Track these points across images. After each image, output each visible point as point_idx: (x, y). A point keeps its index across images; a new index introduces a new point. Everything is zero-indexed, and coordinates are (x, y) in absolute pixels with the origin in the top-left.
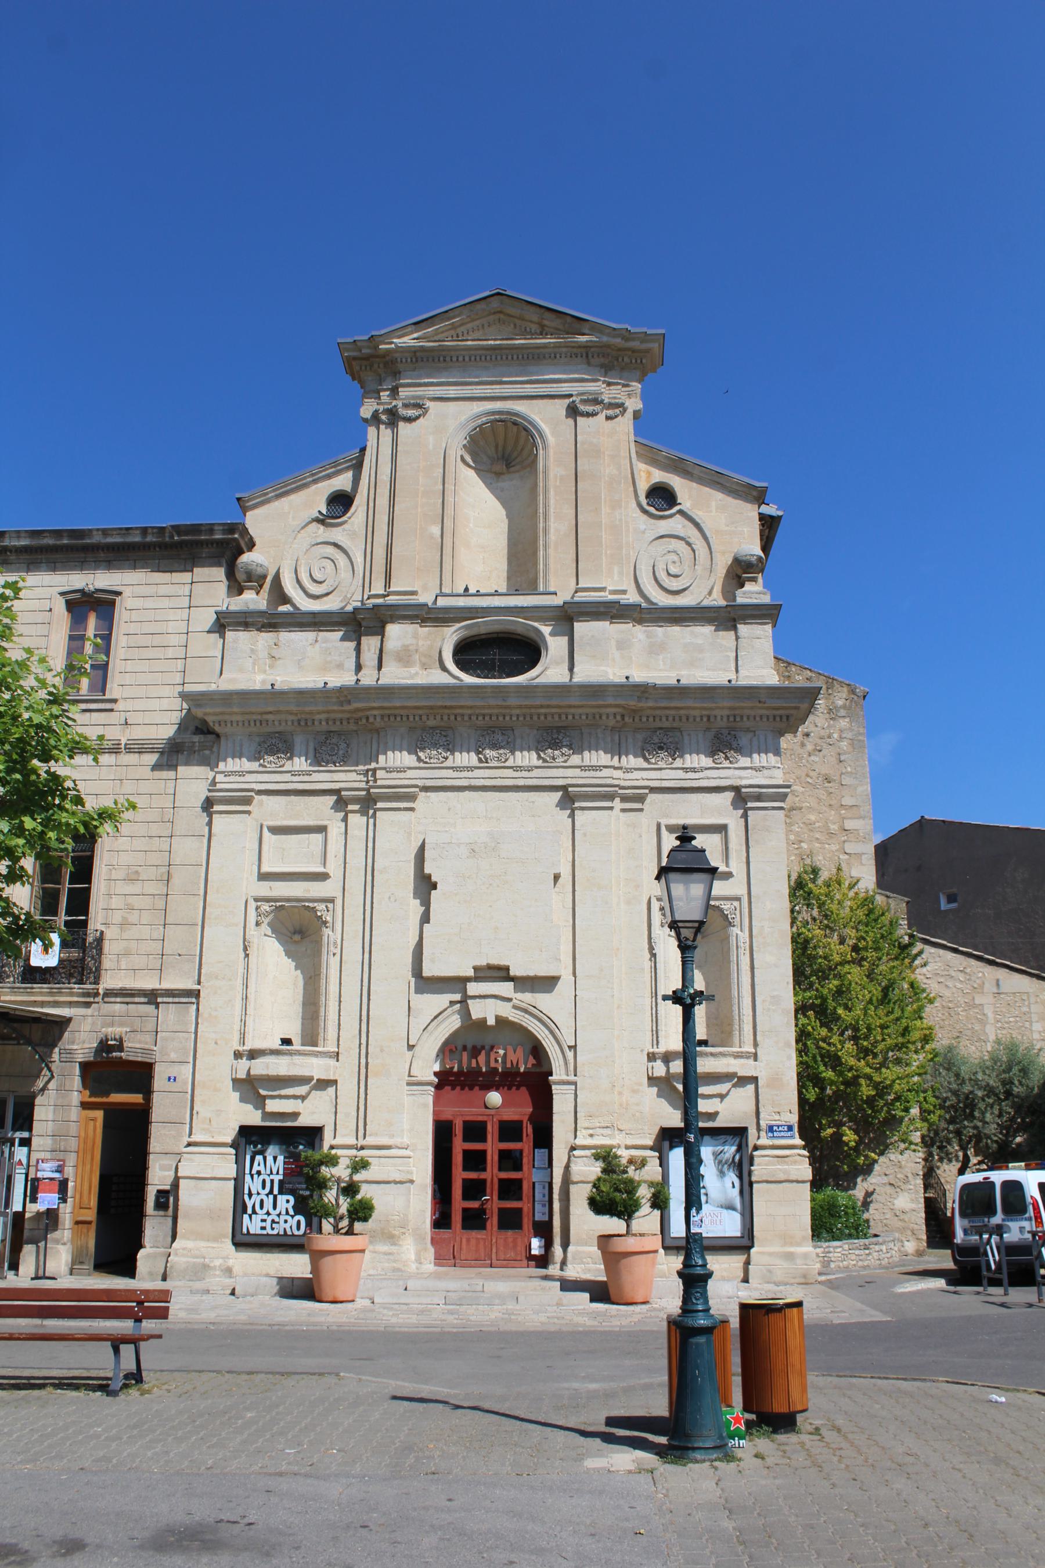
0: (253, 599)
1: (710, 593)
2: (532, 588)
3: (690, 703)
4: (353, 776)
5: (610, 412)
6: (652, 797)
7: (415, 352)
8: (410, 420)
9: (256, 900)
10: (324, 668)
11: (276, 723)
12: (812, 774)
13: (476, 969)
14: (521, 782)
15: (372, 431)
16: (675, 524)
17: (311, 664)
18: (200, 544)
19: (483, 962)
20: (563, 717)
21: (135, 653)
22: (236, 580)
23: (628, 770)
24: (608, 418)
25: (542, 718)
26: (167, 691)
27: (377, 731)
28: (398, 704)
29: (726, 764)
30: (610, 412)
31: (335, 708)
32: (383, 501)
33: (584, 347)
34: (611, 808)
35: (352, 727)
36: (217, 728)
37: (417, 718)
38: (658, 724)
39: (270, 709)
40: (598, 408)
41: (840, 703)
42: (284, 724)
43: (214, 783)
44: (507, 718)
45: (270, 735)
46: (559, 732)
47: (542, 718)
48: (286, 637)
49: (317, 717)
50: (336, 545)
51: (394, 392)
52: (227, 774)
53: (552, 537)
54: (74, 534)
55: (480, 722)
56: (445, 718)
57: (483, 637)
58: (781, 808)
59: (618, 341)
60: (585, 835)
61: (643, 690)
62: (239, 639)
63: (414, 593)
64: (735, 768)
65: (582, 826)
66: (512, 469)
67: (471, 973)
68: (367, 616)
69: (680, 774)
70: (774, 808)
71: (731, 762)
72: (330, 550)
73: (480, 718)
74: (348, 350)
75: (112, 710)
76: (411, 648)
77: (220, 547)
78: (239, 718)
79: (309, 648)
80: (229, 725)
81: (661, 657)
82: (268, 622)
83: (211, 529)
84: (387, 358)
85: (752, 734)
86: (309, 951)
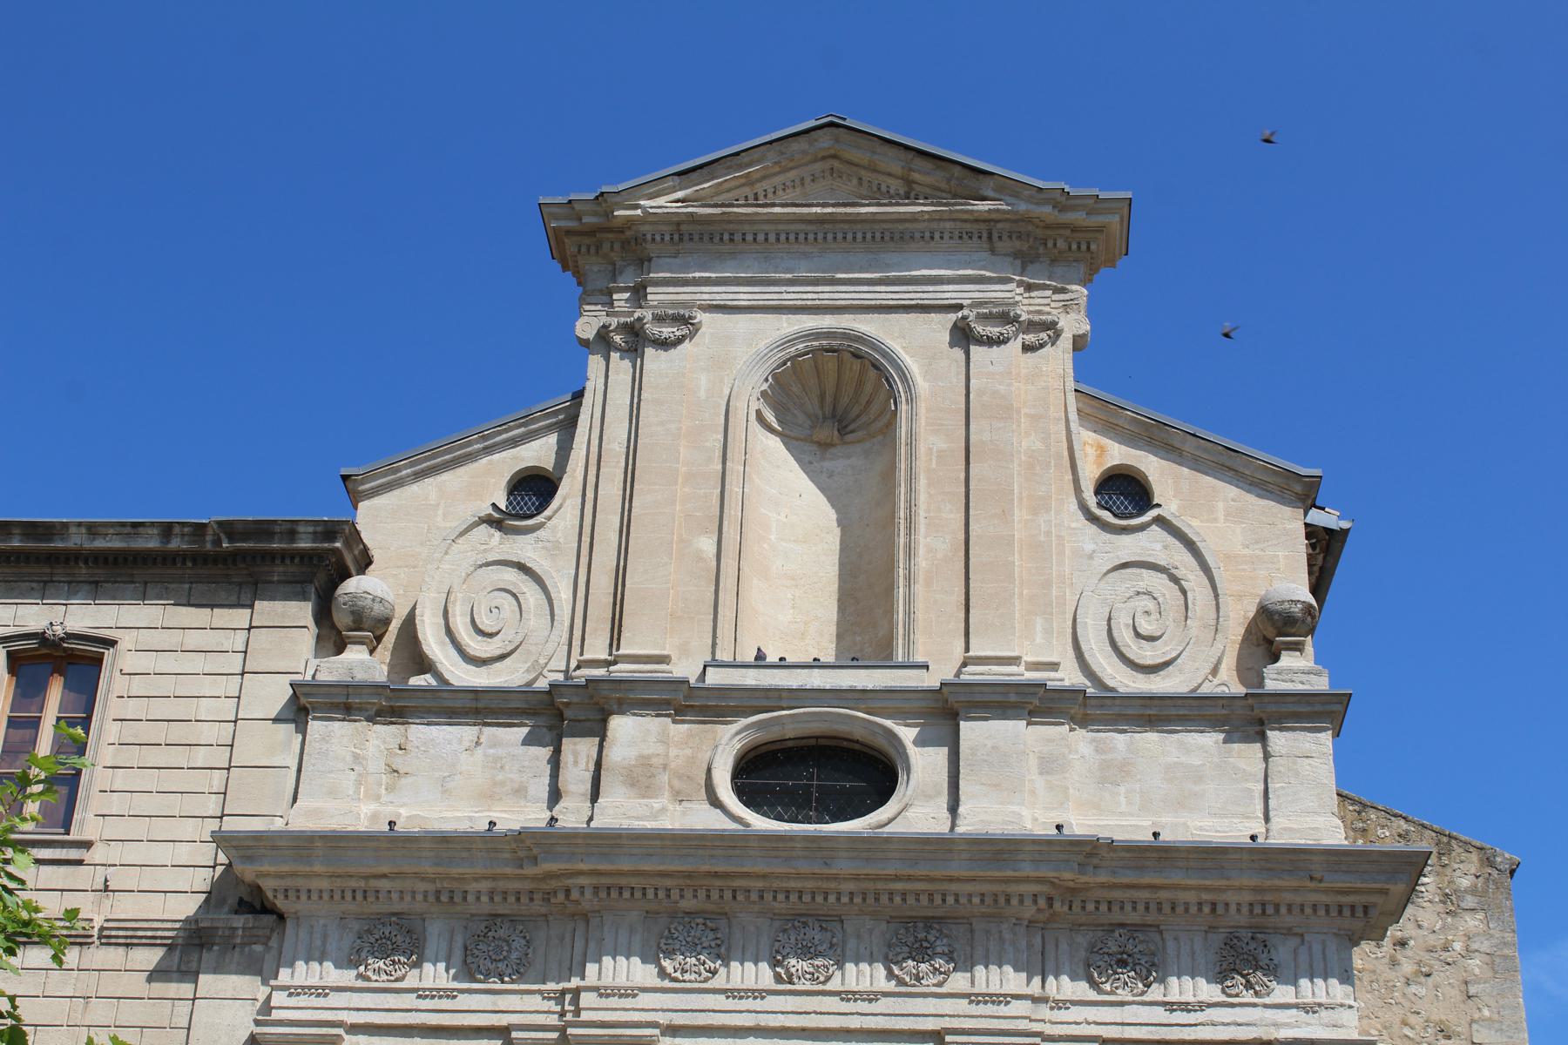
0: (362, 662)
1: (1215, 671)
2: (883, 657)
3: (1177, 878)
4: (535, 1002)
5: (1031, 338)
7: (678, 224)
8: (665, 344)
10: (488, 796)
11: (394, 896)
12: (1413, 1019)
14: (855, 1023)
15: (595, 363)
16: (1151, 544)
17: (463, 786)
18: (271, 556)
20: (938, 899)
21: (133, 756)
22: (333, 626)
23: (1060, 1005)
24: (1027, 348)
25: (898, 899)
26: (189, 829)
27: (585, 917)
28: (626, 866)
29: (1248, 997)
30: (1031, 338)
31: (508, 870)
32: (611, 490)
33: (984, 221)
35: (538, 907)
36: (280, 903)
37: (661, 894)
38: (1117, 917)
39: (385, 869)
40: (1008, 330)
41: (1465, 883)
42: (408, 898)
43: (267, 1007)
44: (832, 899)
45: (381, 919)
46: (928, 928)
47: (898, 899)
48: (419, 733)
49: (472, 887)
50: (522, 568)
51: (639, 294)
52: (293, 991)
53: (922, 562)
54: (33, 530)
55: (780, 905)
56: (715, 895)
57: (790, 744)
59: (1046, 211)
61: (1090, 851)
62: (330, 734)
63: (663, 659)
64: (1266, 1006)
66: (849, 437)
68: (575, 700)
69: (1160, 1014)
71: (1257, 994)
72: (511, 577)
73: (781, 897)
74: (556, 217)
75: (80, 862)
76: (654, 761)
77: (305, 563)
78: (325, 884)
79: (464, 755)
80: (304, 897)
81: (1122, 789)
82: (389, 706)
83: (291, 530)
84: (628, 234)
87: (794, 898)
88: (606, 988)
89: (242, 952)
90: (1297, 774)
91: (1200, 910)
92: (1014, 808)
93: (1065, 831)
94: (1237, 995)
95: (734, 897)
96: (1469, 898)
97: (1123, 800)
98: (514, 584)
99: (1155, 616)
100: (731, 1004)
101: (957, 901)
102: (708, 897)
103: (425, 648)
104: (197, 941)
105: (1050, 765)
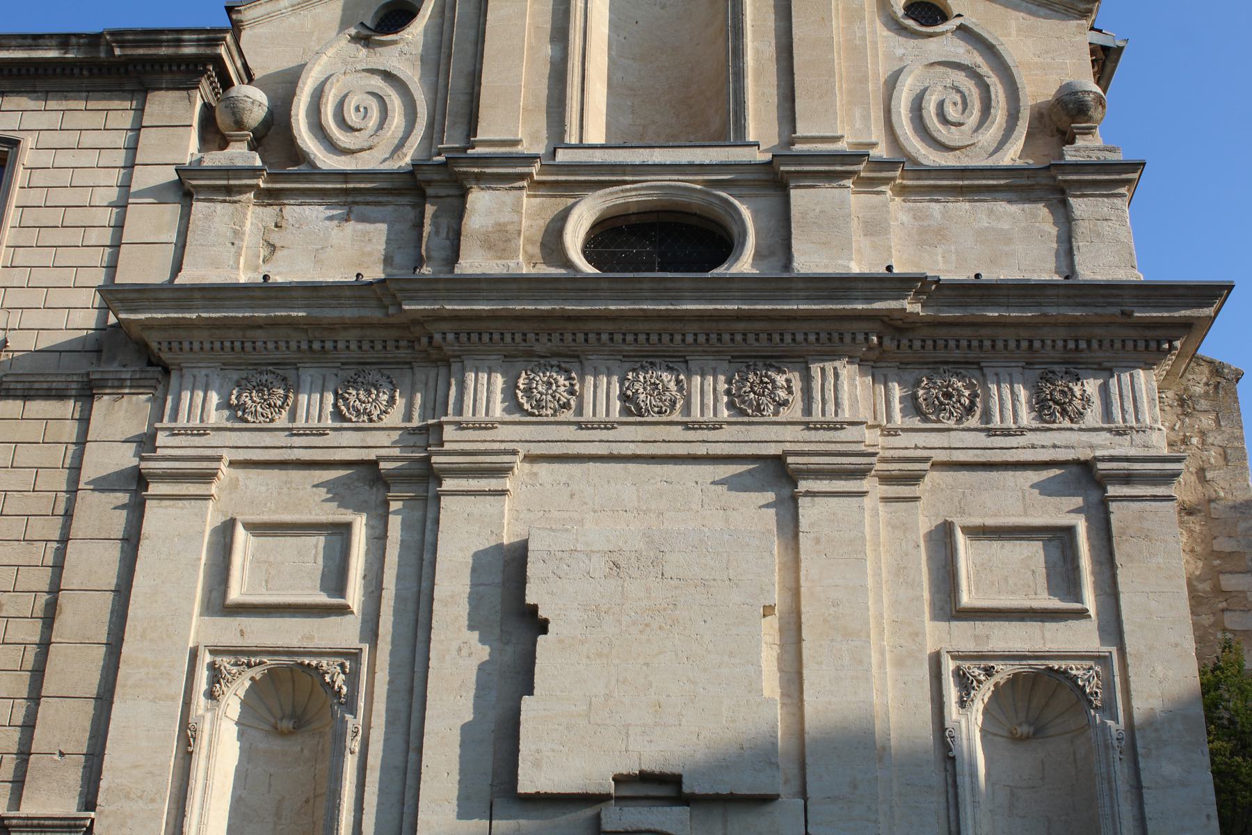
2: (719, 139)
6: (933, 477)
9: (215, 652)
13: (619, 780)
14: (701, 450)
19: (631, 766)
20: (777, 337)
22: (218, 131)
25: (739, 338)
29: (1067, 423)
34: (862, 494)
36: (166, 356)
57: (634, 219)
58: (1169, 498)
60: (817, 541)
63: (516, 143)
64: (1081, 430)
65: (812, 525)
67: (610, 787)
68: (436, 177)
69: (981, 439)
70: (1155, 498)
71: (1072, 421)
72: (377, 83)
76: (509, 227)
81: (939, 250)
83: (176, 36)
85: (1107, 373)
86: (306, 752)
87: (642, 338)
88: (467, 423)
89: (130, 402)
90: (1098, 235)
91: (1018, 347)
92: (840, 262)
93: (895, 271)
94: (1054, 422)
96: (1202, 401)
97: (940, 258)
98: (381, 88)
99: (960, 107)
100: (585, 435)
103: (299, 141)
104: (88, 393)
105: (875, 227)
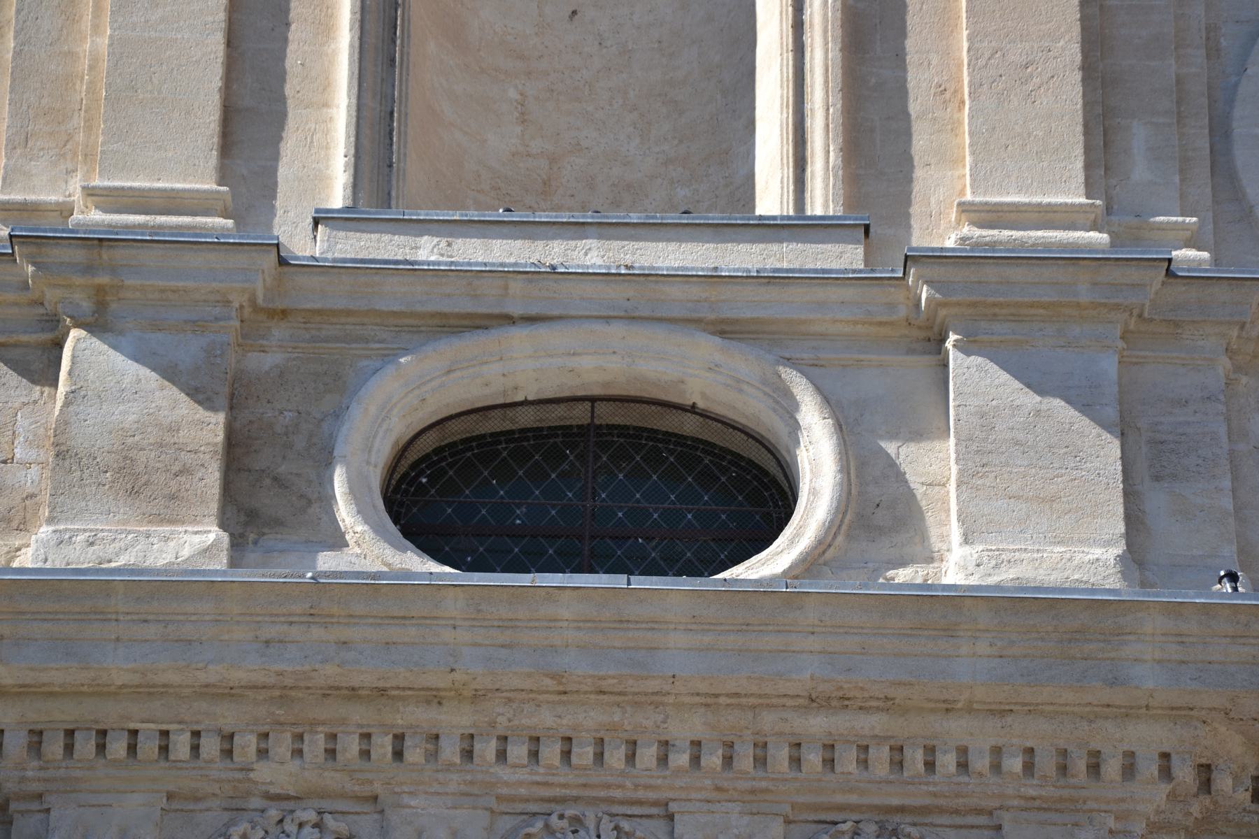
20: (916, 758)
25: (813, 758)
28: (119, 668)
37: (211, 746)
44: (648, 755)
47: (813, 758)
55: (515, 775)
56: (350, 747)
57: (526, 418)
73: (518, 752)
87: (551, 752)
95: (398, 754)
101: (963, 766)
102: (331, 753)
